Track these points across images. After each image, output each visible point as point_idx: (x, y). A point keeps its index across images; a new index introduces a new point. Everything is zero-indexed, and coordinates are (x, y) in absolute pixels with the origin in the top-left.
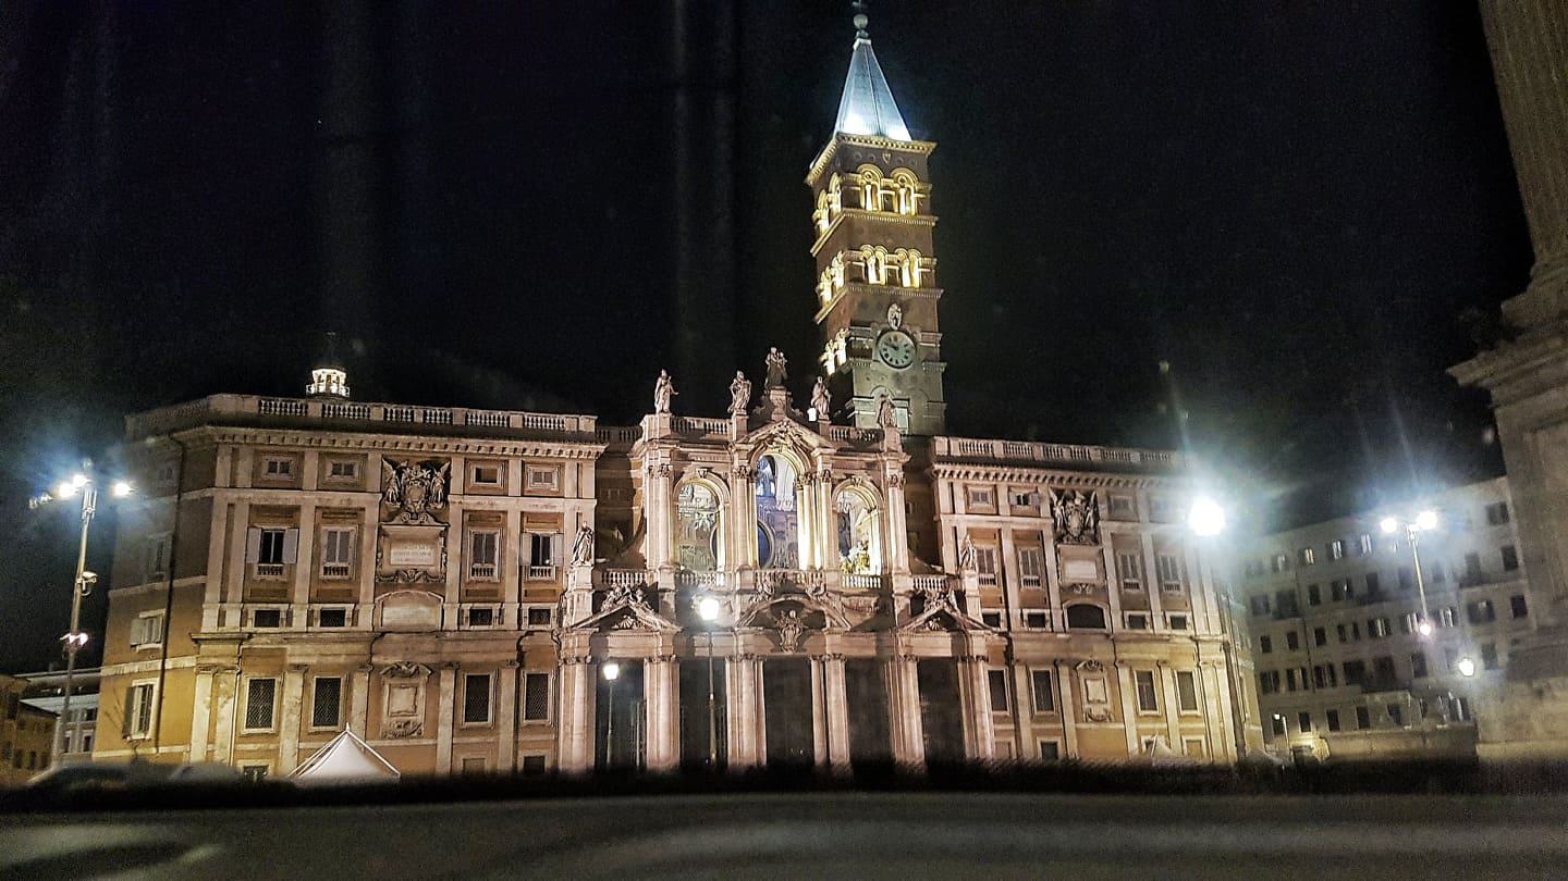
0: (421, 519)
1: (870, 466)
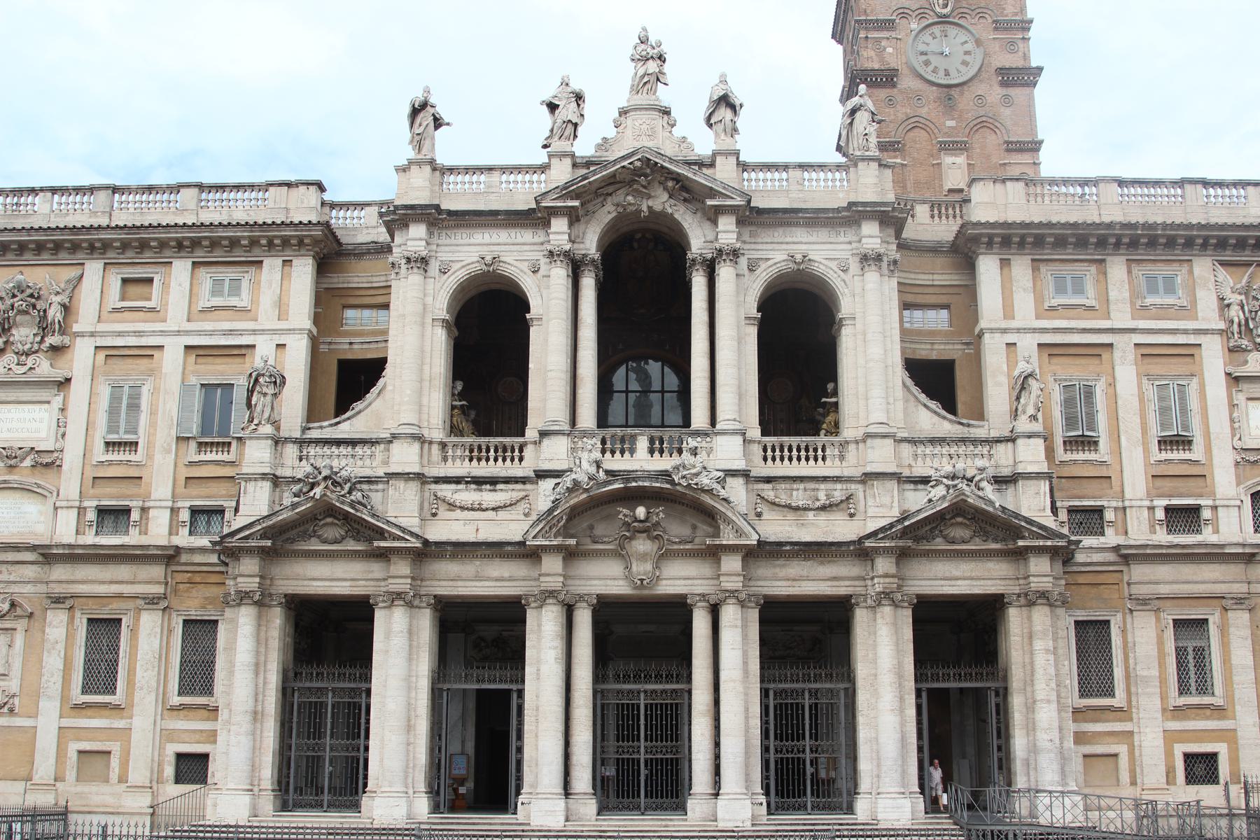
0: (30, 364)
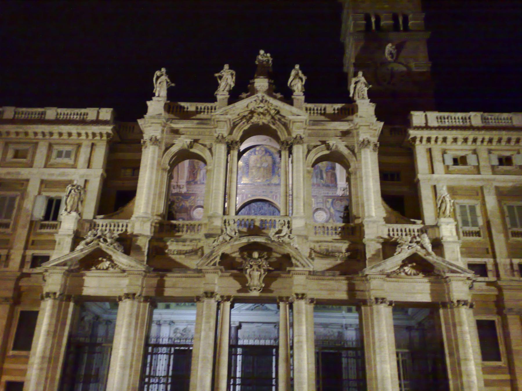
1: (345, 134)
